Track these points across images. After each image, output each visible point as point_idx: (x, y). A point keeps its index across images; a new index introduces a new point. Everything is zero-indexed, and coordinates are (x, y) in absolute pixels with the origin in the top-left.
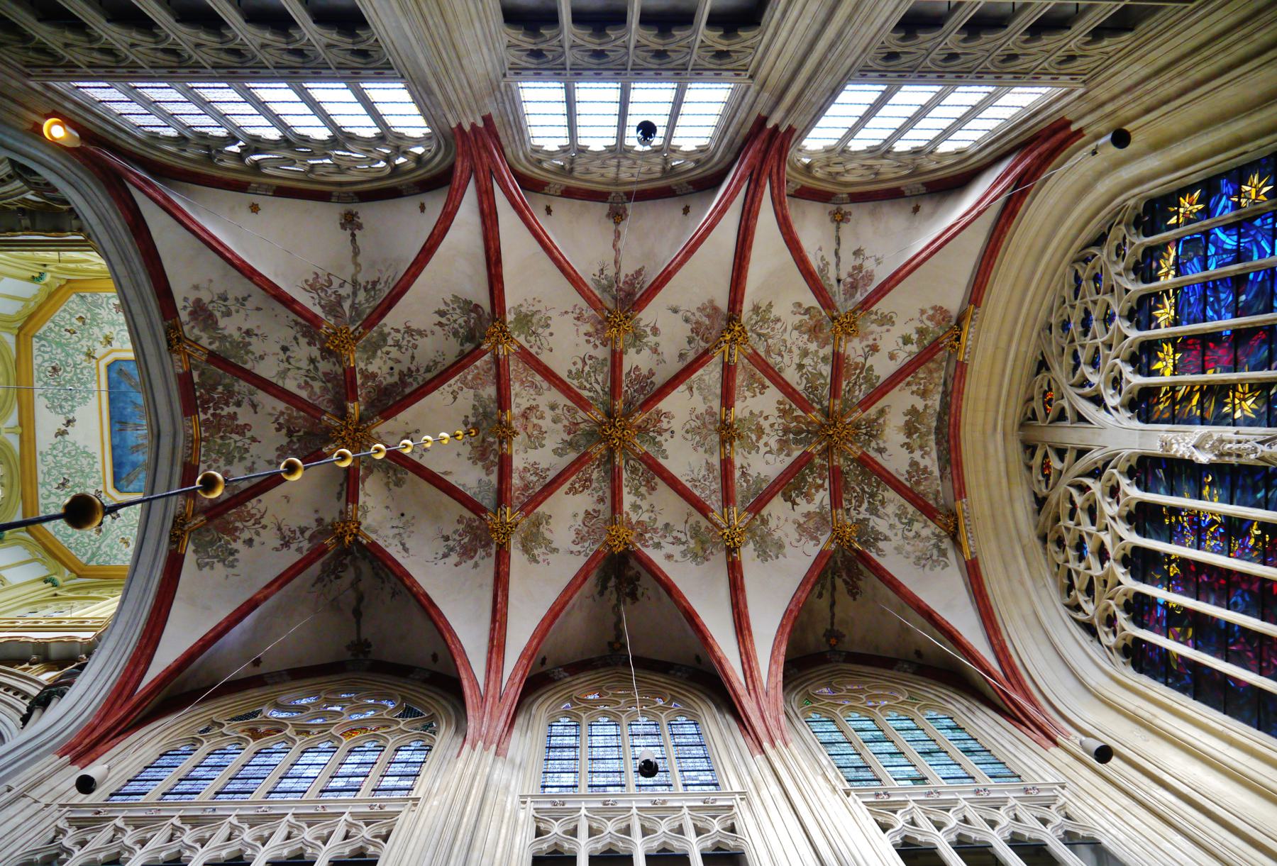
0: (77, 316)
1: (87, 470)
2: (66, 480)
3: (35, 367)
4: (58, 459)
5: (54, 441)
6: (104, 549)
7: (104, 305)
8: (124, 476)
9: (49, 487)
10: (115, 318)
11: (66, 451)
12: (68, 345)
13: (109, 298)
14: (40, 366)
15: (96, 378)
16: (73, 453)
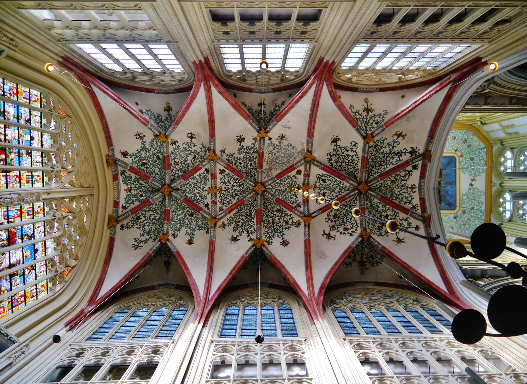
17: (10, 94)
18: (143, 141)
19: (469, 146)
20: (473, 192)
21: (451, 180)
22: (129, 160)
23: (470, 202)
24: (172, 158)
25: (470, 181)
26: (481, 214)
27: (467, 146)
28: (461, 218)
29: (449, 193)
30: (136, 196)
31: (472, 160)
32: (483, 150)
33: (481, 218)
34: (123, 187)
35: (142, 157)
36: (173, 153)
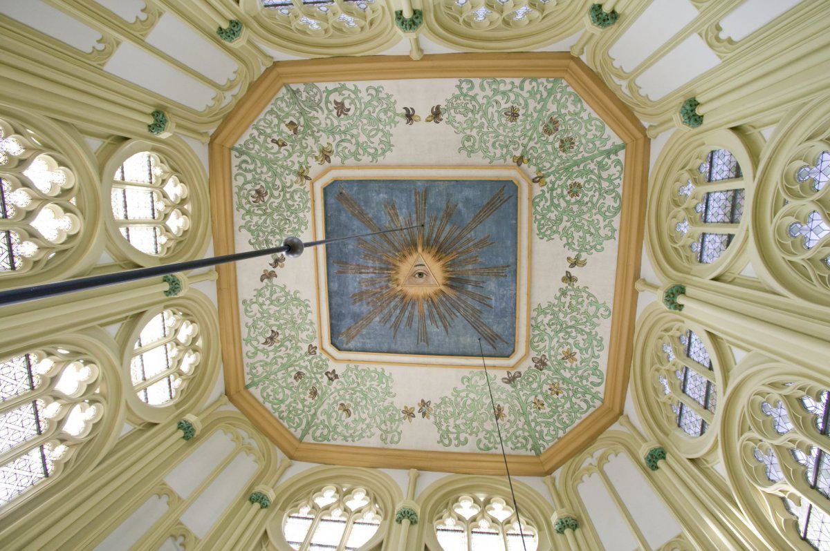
0: (288, 122)
1: (299, 321)
2: (275, 333)
3: (235, 190)
4: (264, 307)
5: (260, 285)
6: (321, 417)
7: (323, 105)
8: (344, 330)
9: (255, 343)
10: (336, 123)
11: (274, 297)
12: (275, 162)
13: (330, 93)
14: (241, 189)
15: (309, 204)
16: (283, 300)
19: (567, 144)
20: (574, 302)
21: (501, 262)
23: (561, 335)
25: (566, 266)
26: (594, 379)
27: (557, 145)
28: (530, 383)
29: (493, 302)
31: (573, 193)
32: (613, 157)
33: (595, 390)
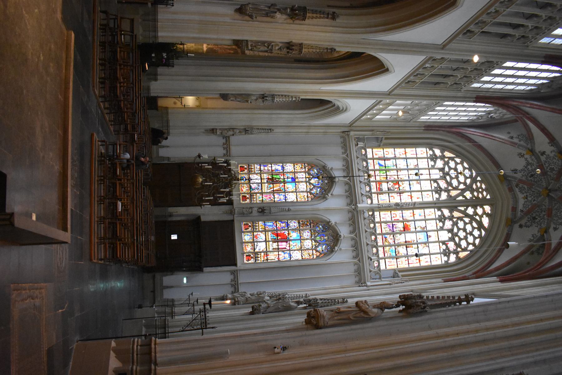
17: (400, 155)
18: (525, 158)
22: (519, 175)
24: (547, 165)
30: (531, 201)
34: (520, 196)
35: (530, 170)
36: (546, 162)
